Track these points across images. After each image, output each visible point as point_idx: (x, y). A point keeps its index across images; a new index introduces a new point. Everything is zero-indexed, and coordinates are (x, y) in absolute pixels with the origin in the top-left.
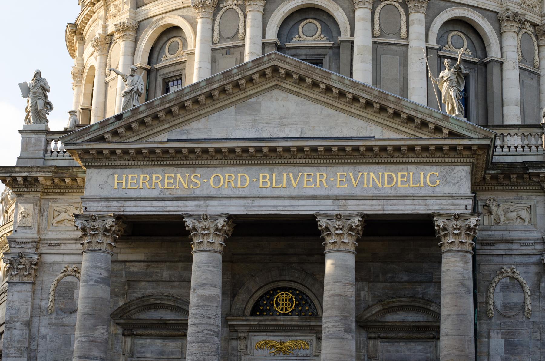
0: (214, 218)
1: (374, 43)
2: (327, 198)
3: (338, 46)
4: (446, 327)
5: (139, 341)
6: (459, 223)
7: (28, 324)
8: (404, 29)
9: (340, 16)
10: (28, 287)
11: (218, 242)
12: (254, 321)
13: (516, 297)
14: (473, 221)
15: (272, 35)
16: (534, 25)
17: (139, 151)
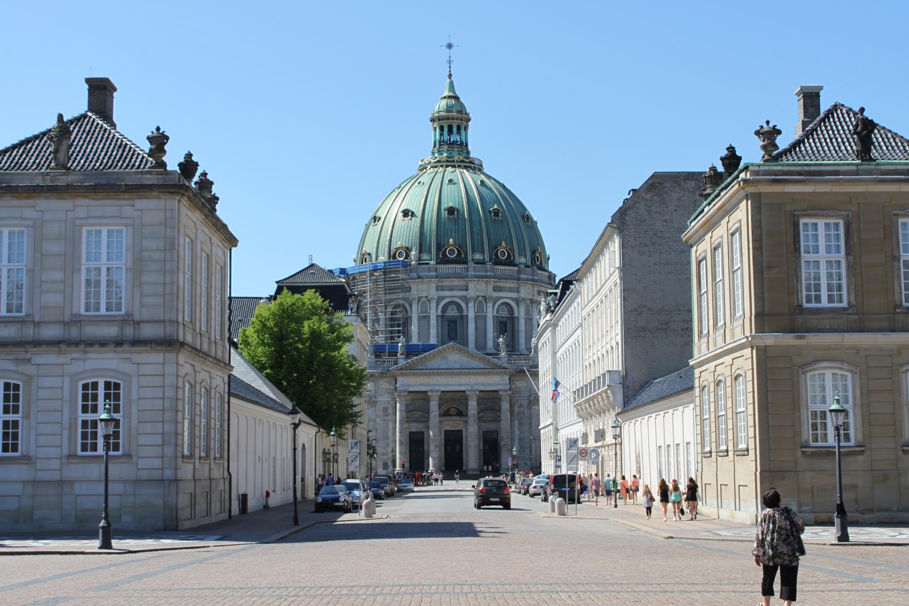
0: (437, 391)
1: (475, 315)
2: (469, 385)
3: (462, 317)
4: (503, 422)
5: (410, 425)
6: (506, 393)
7: (374, 420)
8: (485, 311)
9: (463, 305)
10: (373, 409)
11: (437, 399)
12: (445, 418)
13: (522, 409)
14: (510, 392)
15: (439, 313)
16: (530, 300)
17: (414, 373)
